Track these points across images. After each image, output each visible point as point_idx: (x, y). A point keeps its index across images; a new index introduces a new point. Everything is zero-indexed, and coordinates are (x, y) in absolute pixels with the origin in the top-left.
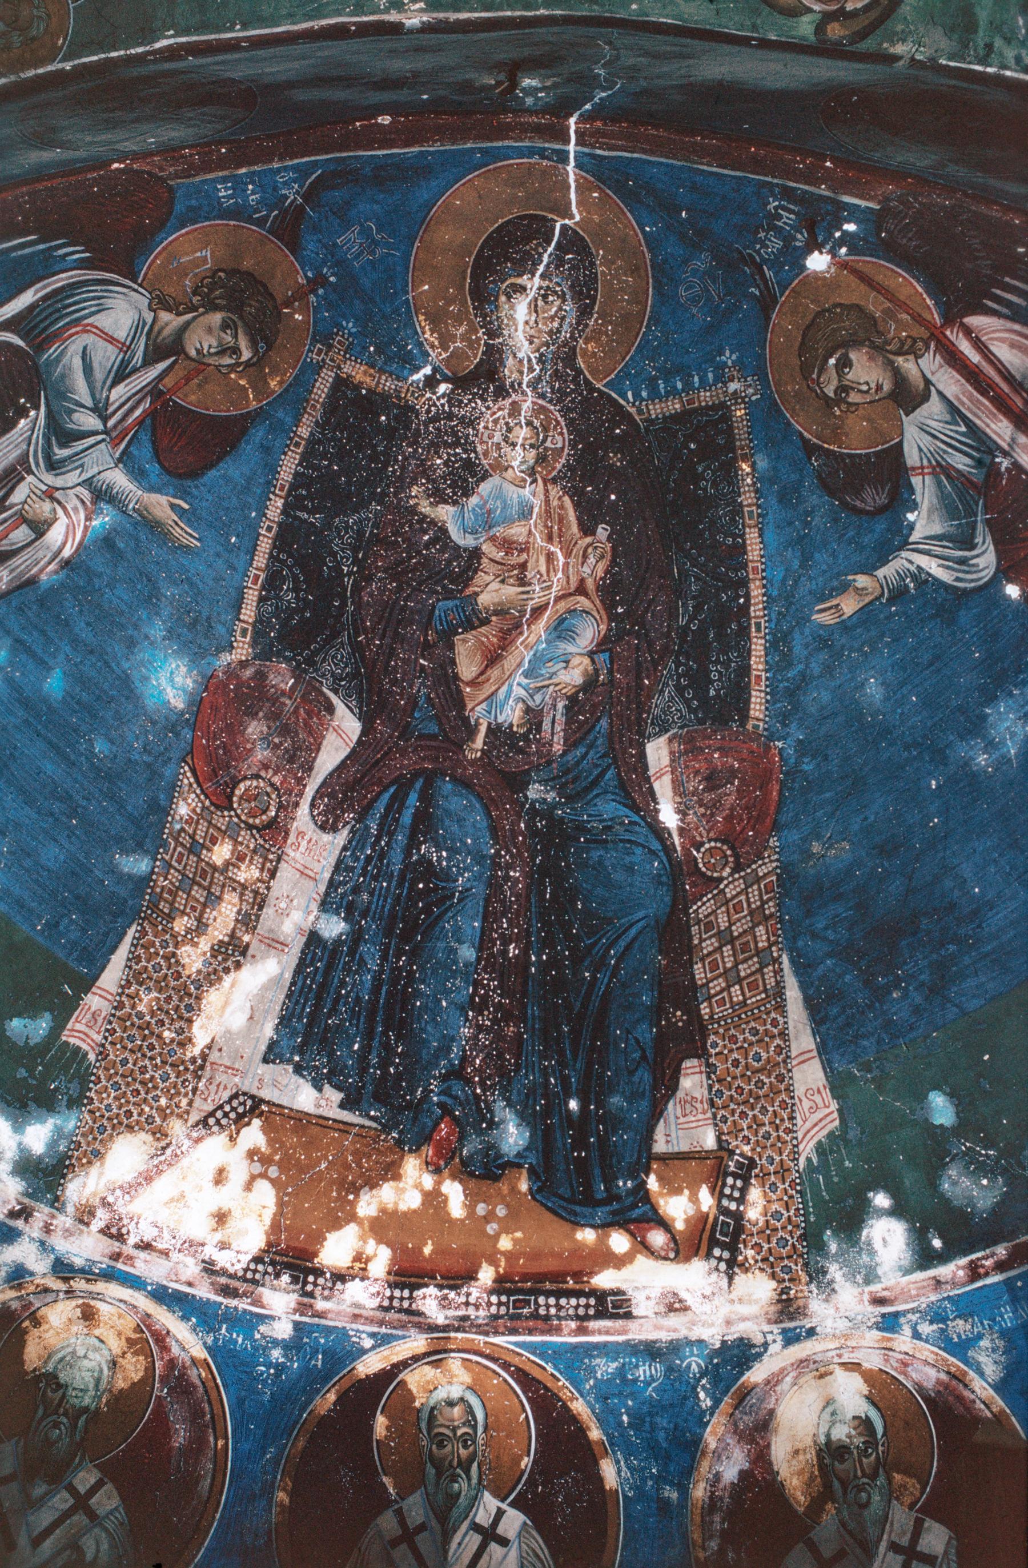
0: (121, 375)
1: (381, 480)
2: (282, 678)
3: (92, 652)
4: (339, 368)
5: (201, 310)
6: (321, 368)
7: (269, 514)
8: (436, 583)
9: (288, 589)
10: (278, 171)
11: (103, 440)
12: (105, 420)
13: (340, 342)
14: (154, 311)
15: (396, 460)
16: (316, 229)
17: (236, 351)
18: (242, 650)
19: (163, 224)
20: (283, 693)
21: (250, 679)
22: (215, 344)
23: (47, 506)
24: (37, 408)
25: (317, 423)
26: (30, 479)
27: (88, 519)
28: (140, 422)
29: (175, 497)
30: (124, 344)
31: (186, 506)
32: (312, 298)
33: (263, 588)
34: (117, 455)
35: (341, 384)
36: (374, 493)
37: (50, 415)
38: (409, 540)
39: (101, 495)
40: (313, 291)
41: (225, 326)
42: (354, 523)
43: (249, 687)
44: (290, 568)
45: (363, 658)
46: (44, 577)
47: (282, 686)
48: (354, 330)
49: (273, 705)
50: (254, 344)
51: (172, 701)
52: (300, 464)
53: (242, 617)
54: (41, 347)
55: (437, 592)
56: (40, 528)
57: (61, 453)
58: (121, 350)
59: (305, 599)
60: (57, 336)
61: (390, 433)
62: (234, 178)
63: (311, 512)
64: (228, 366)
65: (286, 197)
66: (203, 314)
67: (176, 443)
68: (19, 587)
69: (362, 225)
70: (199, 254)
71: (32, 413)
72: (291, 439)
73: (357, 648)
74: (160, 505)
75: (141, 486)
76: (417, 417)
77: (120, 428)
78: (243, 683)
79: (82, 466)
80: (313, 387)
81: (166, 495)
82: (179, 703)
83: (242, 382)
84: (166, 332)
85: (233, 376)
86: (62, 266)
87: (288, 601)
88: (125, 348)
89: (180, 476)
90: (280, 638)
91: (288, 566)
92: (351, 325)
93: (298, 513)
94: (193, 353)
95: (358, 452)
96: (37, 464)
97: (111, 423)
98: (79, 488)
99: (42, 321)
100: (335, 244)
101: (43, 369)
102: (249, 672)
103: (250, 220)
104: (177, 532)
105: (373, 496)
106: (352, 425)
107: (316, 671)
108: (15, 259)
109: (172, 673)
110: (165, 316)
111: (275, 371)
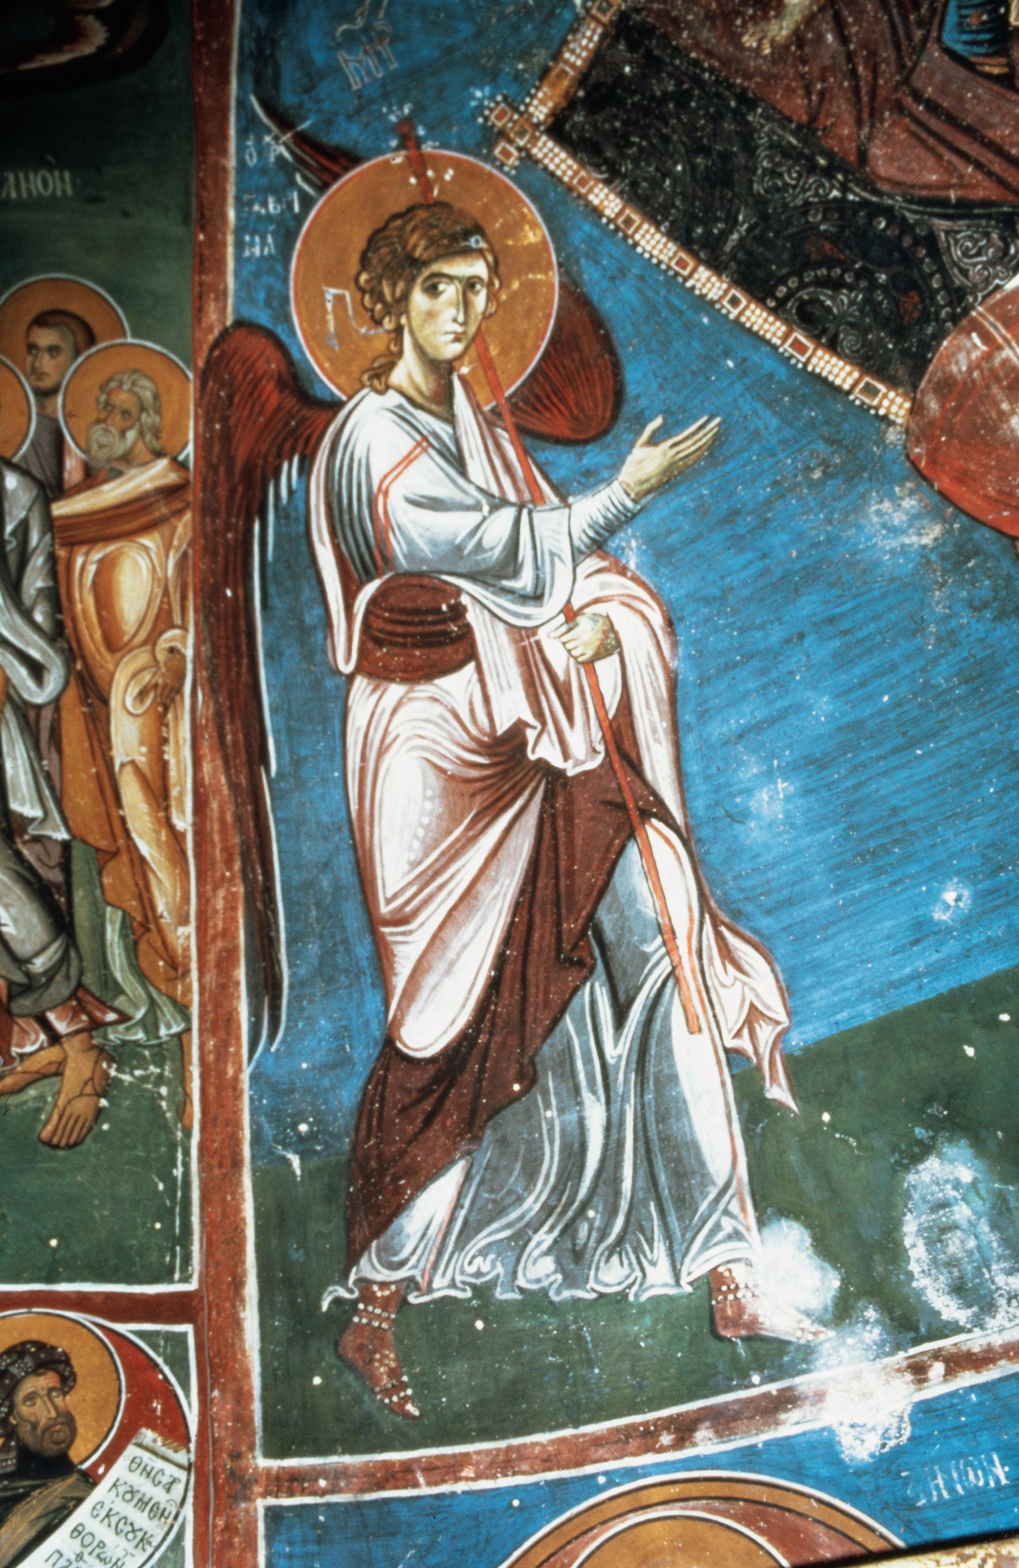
0: (458, 462)
1: (718, 95)
2: (961, 354)
3: (801, 636)
4: (536, 126)
5: (403, 320)
6: (529, 156)
7: (713, 294)
8: (909, 37)
9: (832, 298)
10: (242, 164)
11: (530, 513)
12: (504, 502)
13: (499, 117)
14: (388, 387)
15: (696, 63)
16: (329, 122)
17: (470, 284)
18: (894, 404)
19: (281, 347)
20: (988, 357)
21: (942, 407)
22: (452, 312)
23: (584, 623)
24: (459, 591)
25: (607, 182)
26: (542, 635)
27: (623, 571)
28: (525, 452)
29: (639, 433)
30: (419, 444)
31: (658, 422)
32: (428, 148)
33: (816, 338)
34: (555, 500)
35: (557, 129)
36: (736, 112)
37: (473, 577)
38: (824, 70)
39: (600, 543)
40: (419, 142)
41: (432, 290)
42: (771, 158)
43: (956, 411)
44: (803, 286)
45: (986, 203)
46: (673, 665)
47: (974, 355)
48: (487, 90)
49: (998, 380)
50: (467, 252)
51: (926, 540)
52: (658, 225)
53: (846, 387)
54: (388, 560)
55: (925, 39)
56: (611, 644)
57: (525, 581)
58: (425, 450)
59: (858, 275)
60: (382, 530)
61: (651, 64)
62: (240, 230)
63: (732, 223)
64: (488, 299)
65: (280, 158)
66: (409, 318)
67: (570, 409)
68: (673, 701)
69: (339, 46)
70: (329, 306)
71: (465, 600)
72: (617, 229)
73: (964, 210)
74: (644, 461)
75: (608, 482)
76: (637, 11)
77: (522, 485)
78: (944, 417)
79: (552, 554)
80: (552, 174)
81: (632, 445)
82: (932, 534)
83: (516, 285)
84: (419, 378)
85: (504, 297)
86: (300, 496)
87: (852, 303)
88: (425, 441)
89: (615, 417)
90: (899, 333)
91: (799, 289)
92: (478, 94)
93: (728, 248)
94: (458, 348)
95: (666, 123)
96: (527, 617)
97: (512, 496)
98: (579, 570)
99: (358, 547)
100: (359, 95)
101: (415, 568)
102: (933, 405)
103: (300, 219)
104: (688, 448)
105: (739, 116)
106: (624, 123)
107: (974, 292)
108: (276, 557)
109: (884, 526)
110: (398, 376)
111: (513, 229)
